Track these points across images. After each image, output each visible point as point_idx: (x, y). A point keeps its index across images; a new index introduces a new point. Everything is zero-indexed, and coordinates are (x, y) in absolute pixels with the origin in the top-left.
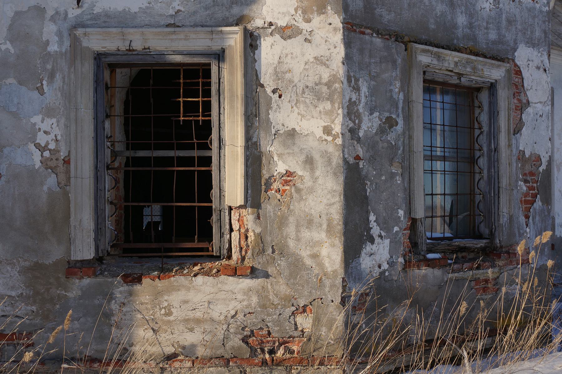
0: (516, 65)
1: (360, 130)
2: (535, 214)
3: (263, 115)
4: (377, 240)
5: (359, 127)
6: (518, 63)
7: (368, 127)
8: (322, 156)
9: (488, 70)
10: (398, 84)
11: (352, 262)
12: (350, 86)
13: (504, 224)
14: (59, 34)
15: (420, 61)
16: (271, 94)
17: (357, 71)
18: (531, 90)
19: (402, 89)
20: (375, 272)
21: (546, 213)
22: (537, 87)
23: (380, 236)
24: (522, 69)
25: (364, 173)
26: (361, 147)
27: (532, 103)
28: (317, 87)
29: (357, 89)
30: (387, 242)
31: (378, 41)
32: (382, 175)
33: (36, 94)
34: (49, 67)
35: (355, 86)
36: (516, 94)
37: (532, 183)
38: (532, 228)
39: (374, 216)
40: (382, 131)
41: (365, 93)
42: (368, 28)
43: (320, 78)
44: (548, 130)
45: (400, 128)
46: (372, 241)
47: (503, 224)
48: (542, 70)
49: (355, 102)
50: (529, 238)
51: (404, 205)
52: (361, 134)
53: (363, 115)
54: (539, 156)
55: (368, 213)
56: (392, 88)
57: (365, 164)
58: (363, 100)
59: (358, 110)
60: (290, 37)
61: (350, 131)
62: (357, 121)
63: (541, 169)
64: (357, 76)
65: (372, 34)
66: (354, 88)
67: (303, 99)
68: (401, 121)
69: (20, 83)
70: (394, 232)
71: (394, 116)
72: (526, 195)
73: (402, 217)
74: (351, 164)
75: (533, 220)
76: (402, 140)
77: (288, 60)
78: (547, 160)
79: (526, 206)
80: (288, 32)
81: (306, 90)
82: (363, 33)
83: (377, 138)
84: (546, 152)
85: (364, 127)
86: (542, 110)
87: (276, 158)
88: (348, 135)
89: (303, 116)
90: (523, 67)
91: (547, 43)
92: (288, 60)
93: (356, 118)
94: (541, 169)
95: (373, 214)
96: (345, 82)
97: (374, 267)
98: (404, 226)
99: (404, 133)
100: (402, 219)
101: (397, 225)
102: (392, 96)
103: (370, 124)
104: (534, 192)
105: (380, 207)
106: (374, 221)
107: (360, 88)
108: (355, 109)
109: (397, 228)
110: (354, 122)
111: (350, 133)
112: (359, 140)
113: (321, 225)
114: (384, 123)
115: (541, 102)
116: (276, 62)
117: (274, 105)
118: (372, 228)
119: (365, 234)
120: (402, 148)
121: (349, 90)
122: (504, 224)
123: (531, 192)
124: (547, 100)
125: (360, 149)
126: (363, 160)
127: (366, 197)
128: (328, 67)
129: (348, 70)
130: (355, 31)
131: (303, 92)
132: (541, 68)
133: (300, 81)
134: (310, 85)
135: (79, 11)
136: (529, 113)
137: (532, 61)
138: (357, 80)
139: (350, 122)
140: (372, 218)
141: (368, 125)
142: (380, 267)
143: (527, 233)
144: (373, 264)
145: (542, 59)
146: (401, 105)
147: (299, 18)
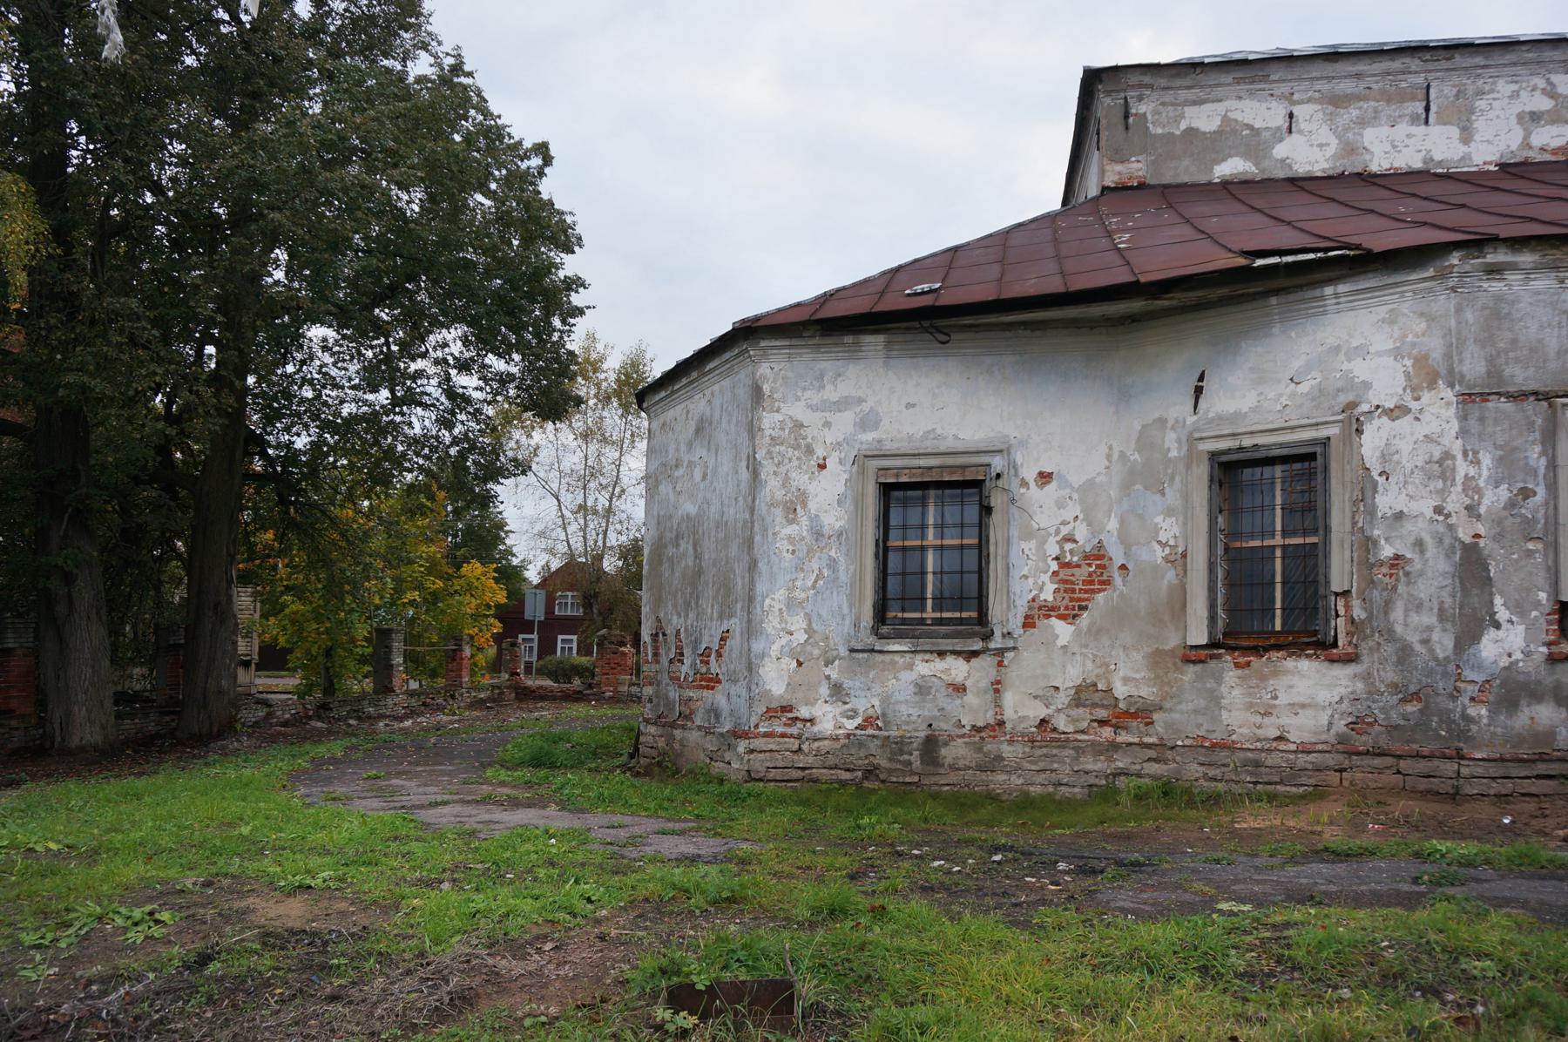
10: (1538, 449)
14: (1179, 441)
16: (1377, 478)
19: (1543, 453)
29: (1476, 462)
33: (1158, 497)
34: (1170, 471)
40: (1511, 504)
49: (1473, 477)
52: (1482, 510)
56: (1528, 454)
58: (1485, 473)
60: (1397, 418)
61: (1467, 508)
62: (1476, 497)
64: (1477, 448)
69: (1146, 488)
71: (1530, 486)
77: (1396, 441)
80: (1396, 413)
82: (1488, 400)
83: (1506, 513)
85: (1486, 502)
89: (1411, 497)
92: (1396, 441)
99: (1547, 503)
102: (1527, 464)
112: (1479, 517)
113: (1431, 609)
117: (1380, 489)
121: (1465, 465)
127: (1490, 579)
130: (1474, 401)
134: (1420, 464)
135: (1195, 418)
138: (1476, 453)
146: (1542, 471)
147: (1408, 397)
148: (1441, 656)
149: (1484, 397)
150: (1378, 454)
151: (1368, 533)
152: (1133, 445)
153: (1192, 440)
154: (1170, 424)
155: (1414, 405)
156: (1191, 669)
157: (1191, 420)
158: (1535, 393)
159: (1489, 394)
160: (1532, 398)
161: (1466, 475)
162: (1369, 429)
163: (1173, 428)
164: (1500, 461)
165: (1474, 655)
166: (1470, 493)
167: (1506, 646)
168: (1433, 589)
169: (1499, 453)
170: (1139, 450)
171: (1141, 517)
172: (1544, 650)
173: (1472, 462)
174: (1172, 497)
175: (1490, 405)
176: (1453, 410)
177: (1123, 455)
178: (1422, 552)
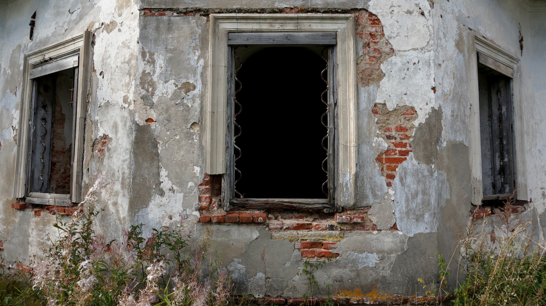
0: (371, 14)
1: (153, 97)
2: (405, 174)
3: (94, 94)
4: (167, 193)
5: (153, 94)
6: (374, 12)
7: (163, 94)
8: (121, 121)
9: (319, 25)
11: (139, 211)
12: (144, 60)
13: (344, 184)
15: (223, 29)
16: (99, 76)
17: (153, 46)
18: (398, 38)
20: (165, 222)
21: (426, 173)
22: (408, 32)
23: (172, 190)
24: (380, 17)
25: (156, 133)
26: (154, 111)
27: (399, 51)
28: (122, 66)
29: (152, 62)
30: (180, 196)
31: (176, 19)
32: (176, 135)
34: (19, 79)
35: (150, 60)
36: (372, 44)
37: (401, 139)
38: (398, 191)
39: (166, 171)
40: (175, 95)
41: (160, 64)
42: (167, 9)
43: (125, 58)
44: (429, 79)
45: (197, 92)
46: (162, 193)
47: (343, 184)
48: (415, 13)
49: (149, 73)
50: (393, 201)
51: (201, 162)
52: (155, 100)
53: (157, 84)
54: (413, 108)
55: (159, 168)
56: (190, 56)
57: (157, 125)
59: (152, 79)
60: (111, 31)
61: (142, 98)
62: (150, 89)
63: (416, 123)
64: (152, 51)
65: (173, 14)
66: (148, 62)
67: (114, 76)
68: (199, 86)
70: (189, 186)
71: (191, 82)
72: (387, 152)
73: (198, 173)
74: (142, 126)
75: (401, 180)
76: (200, 102)
77: (109, 49)
78: (427, 112)
79: (387, 164)
80: (110, 28)
81: (116, 69)
82: (164, 15)
85: (158, 93)
87: (99, 125)
88: (140, 101)
90: (383, 15)
93: (149, 87)
95: (164, 170)
96: (140, 57)
97: (163, 218)
98: (200, 181)
100: (198, 175)
101: (192, 180)
102: (189, 64)
103: (165, 90)
104: (404, 149)
105: (172, 163)
106: (166, 176)
107: (155, 61)
108: (149, 79)
109: (192, 183)
110: (148, 91)
111: (142, 100)
112: (152, 106)
114: (179, 89)
115: (414, 49)
116: (103, 52)
117: (100, 85)
118: (162, 182)
119: (154, 187)
120: (199, 110)
121: (143, 63)
122: (344, 184)
123: (399, 149)
124: (426, 46)
125: (153, 112)
126: (155, 122)
128: (129, 48)
129: (143, 48)
130: (153, 15)
131: (115, 71)
132: (415, 12)
133: (114, 63)
134: (119, 64)
135: (32, 43)
136: (393, 62)
137: (399, 6)
138: (152, 55)
139: (142, 90)
140: (164, 173)
141: (162, 91)
142: (171, 218)
143: (390, 196)
144: (163, 215)
146: (200, 70)
147: (116, 15)
148: (122, 216)
149: (162, 11)
150: (101, 59)
151: (93, 119)
152: (8, 64)
153: (26, 58)
154: (23, 47)
155: (118, 20)
156: (20, 214)
157: (31, 44)
158: (198, 10)
159: (165, 10)
160: (198, 15)
161: (144, 72)
162: (98, 41)
163: (23, 51)
164: (169, 61)
165: (143, 216)
166: (146, 86)
167: (168, 210)
168: (120, 163)
169: (169, 55)
170: (10, 67)
171: (8, 110)
172: (197, 213)
173: (148, 62)
174: (18, 99)
175: (165, 18)
176: (137, 21)
177: (5, 71)
178: (116, 133)
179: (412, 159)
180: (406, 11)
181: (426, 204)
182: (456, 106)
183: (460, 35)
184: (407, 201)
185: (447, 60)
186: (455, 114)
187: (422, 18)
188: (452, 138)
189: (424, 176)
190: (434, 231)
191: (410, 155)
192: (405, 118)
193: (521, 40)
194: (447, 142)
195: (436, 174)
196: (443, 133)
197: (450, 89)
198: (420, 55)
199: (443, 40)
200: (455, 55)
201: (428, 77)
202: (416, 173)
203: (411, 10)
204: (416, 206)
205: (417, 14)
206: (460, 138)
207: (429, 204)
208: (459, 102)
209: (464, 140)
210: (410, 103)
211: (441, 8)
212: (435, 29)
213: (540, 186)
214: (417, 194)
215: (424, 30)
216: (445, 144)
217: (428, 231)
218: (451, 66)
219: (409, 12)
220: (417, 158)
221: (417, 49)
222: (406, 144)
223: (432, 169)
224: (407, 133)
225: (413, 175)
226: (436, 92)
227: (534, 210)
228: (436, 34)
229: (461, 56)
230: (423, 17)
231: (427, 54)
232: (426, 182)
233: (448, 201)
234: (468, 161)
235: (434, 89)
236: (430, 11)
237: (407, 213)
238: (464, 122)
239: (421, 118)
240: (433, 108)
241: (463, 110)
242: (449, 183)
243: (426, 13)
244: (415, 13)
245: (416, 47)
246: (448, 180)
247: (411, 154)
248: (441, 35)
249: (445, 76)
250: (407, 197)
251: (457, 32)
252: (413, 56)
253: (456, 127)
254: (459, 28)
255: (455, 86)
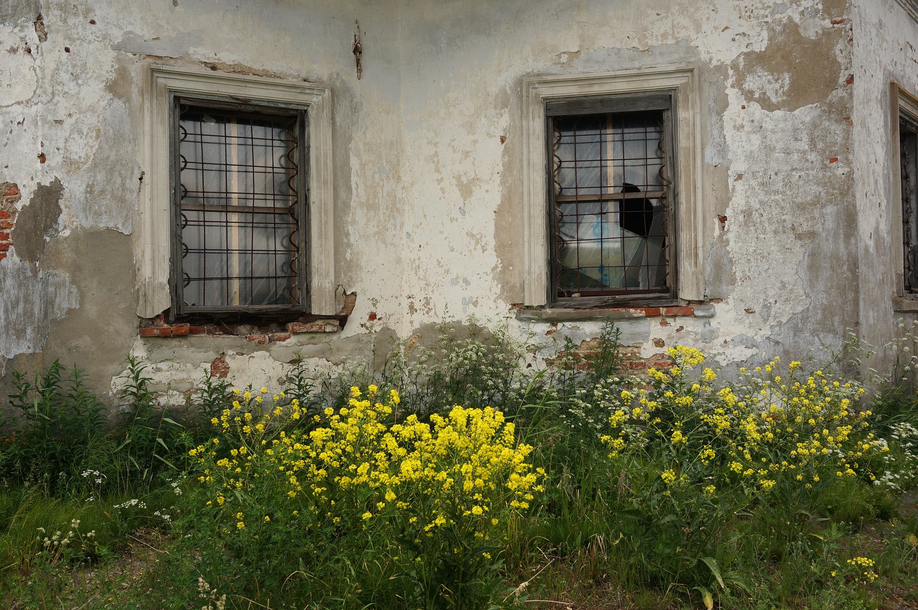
21: (30, 274)
22: (11, 80)
44: (35, 143)
48: (21, 51)
54: (15, 185)
63: (19, 206)
78: (32, 190)
84: (30, 177)
86: (23, 114)
91: (33, 6)
94: (19, 206)
115: (18, 103)
124: (33, 97)
145: (22, 35)
179: (12, 255)
180: (9, 49)
181: (28, 314)
182: (100, 177)
183: (123, 73)
184: (6, 311)
185: (80, 113)
186: (97, 189)
187: (27, 59)
188: (88, 223)
189: (26, 278)
190: (38, 351)
191: (10, 251)
192: (7, 200)
193: (357, 50)
194: (72, 230)
195: (40, 275)
196: (63, 218)
197: (87, 154)
198: (26, 111)
199: (72, 85)
200: (103, 104)
201: (35, 139)
202: (20, 271)
203: (15, 47)
204: (17, 318)
205: (22, 51)
206: (104, 223)
207: (32, 314)
208: (111, 171)
209: (120, 226)
210: (12, 178)
211: (68, 37)
212: (46, 71)
213: (407, 292)
214: (17, 302)
215: (30, 75)
216: (67, 233)
217: (30, 351)
218: (92, 120)
219: (13, 50)
220: (19, 254)
221: (22, 102)
222: (8, 234)
223: (36, 268)
224: (9, 220)
225: (14, 277)
226: (47, 163)
227: (386, 330)
228: (49, 77)
229: (118, 103)
230: (30, 56)
231: (34, 108)
232: (28, 286)
233: (70, 311)
234: (130, 254)
235: (42, 158)
236: (38, 47)
237: (7, 327)
238: (122, 200)
239: (25, 199)
240: (39, 184)
241: (119, 181)
242: (79, 287)
243: (33, 51)
244: (21, 51)
245: (20, 100)
246: (73, 282)
247: (12, 248)
248: (65, 76)
249: (76, 136)
250: (6, 305)
251: (112, 66)
252: (17, 112)
253: (99, 207)
254: (118, 60)
255: (100, 148)
